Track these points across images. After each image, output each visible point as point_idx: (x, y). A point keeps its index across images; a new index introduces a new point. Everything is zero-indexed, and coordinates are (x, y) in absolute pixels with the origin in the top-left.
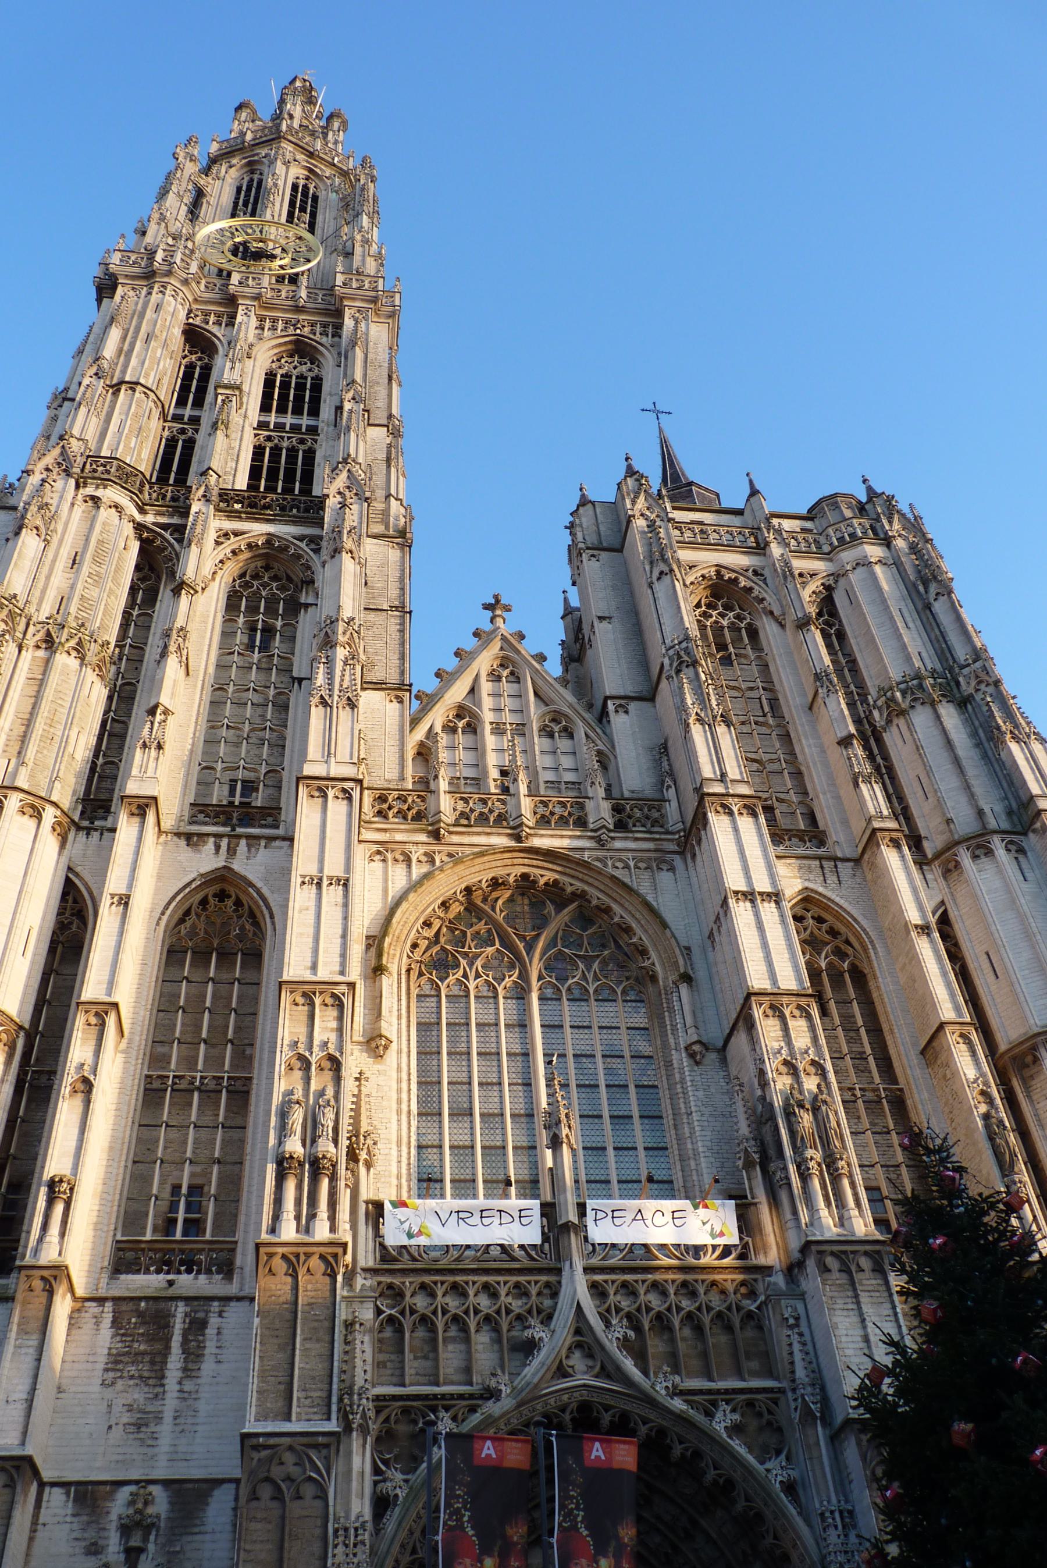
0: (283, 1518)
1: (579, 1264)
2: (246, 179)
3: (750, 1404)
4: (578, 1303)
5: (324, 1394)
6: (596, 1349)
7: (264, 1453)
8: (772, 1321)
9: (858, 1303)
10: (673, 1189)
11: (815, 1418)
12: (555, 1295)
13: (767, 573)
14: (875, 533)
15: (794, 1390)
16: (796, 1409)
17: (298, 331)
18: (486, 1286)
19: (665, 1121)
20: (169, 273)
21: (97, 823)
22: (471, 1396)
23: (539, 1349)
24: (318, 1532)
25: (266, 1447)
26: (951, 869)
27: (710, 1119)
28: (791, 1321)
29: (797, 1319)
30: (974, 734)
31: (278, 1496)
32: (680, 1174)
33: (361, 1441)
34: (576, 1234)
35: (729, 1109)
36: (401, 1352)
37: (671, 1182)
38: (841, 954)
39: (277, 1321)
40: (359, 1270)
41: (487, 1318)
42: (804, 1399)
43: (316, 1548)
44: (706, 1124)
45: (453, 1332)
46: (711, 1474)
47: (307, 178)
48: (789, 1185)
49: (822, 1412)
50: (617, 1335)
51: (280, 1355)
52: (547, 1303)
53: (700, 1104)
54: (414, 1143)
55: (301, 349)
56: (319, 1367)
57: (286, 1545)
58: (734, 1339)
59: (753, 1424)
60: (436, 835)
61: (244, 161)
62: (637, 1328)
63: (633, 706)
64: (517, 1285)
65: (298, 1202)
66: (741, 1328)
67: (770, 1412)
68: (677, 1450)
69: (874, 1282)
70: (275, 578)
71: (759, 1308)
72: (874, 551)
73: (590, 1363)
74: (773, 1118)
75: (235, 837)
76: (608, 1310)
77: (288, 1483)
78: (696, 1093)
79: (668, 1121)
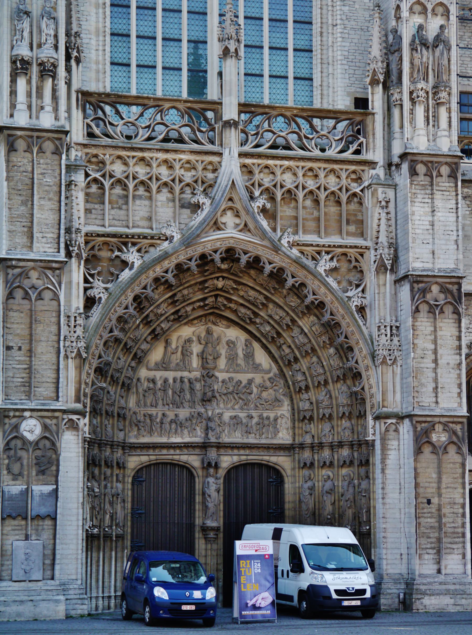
0: (31, 310)
1: (236, 150)
3: (345, 254)
4: (233, 181)
5: (56, 236)
6: (242, 213)
7: (17, 271)
8: (368, 201)
9: (432, 199)
10: (312, 86)
11: (386, 269)
12: (215, 170)
15: (376, 250)
16: (375, 262)
18: (166, 161)
19: (314, 27)
22: (152, 238)
23: (202, 210)
24: (54, 320)
25: (16, 267)
27: (350, 32)
28: (383, 203)
29: (387, 202)
31: (27, 296)
32: (319, 74)
33: (77, 264)
34: (236, 128)
35: (367, 24)
36: (103, 203)
37: (311, 79)
39: (19, 184)
40: (73, 145)
41: (166, 184)
42: (381, 256)
43: (54, 329)
44: (346, 36)
45: (141, 191)
46: (311, 298)
48: (401, 106)
49: (392, 266)
50: (258, 204)
51: (23, 208)
52: (210, 176)
53: (344, 18)
54: (108, 31)
56: (51, 217)
57: (34, 326)
58: (341, 210)
59: (344, 266)
62: (272, 199)
64: (188, 162)
65: (29, 95)
66: (347, 203)
67: (357, 260)
68: (290, 282)
69: (447, 184)
71: (362, 191)
73: (237, 221)
74: (399, 50)
76: (253, 185)
77: (33, 289)
78: (343, 8)
79: (316, 27)
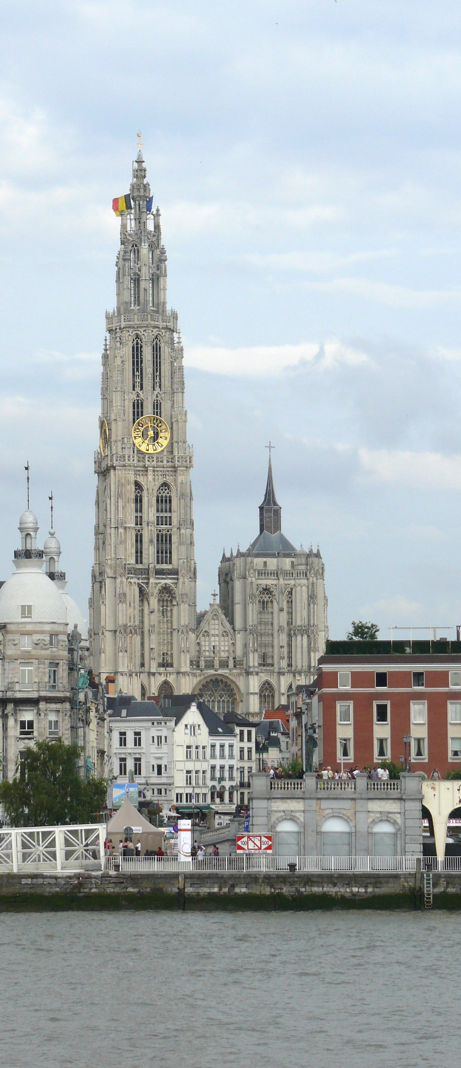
2: (135, 342)
13: (277, 586)
14: (306, 576)
17: (165, 479)
20: (130, 466)
21: (143, 668)
26: (294, 676)
30: (308, 645)
38: (270, 692)
47: (156, 338)
55: (165, 485)
60: (201, 671)
61: (134, 333)
63: (241, 632)
70: (167, 593)
72: (304, 582)
75: (167, 673)
